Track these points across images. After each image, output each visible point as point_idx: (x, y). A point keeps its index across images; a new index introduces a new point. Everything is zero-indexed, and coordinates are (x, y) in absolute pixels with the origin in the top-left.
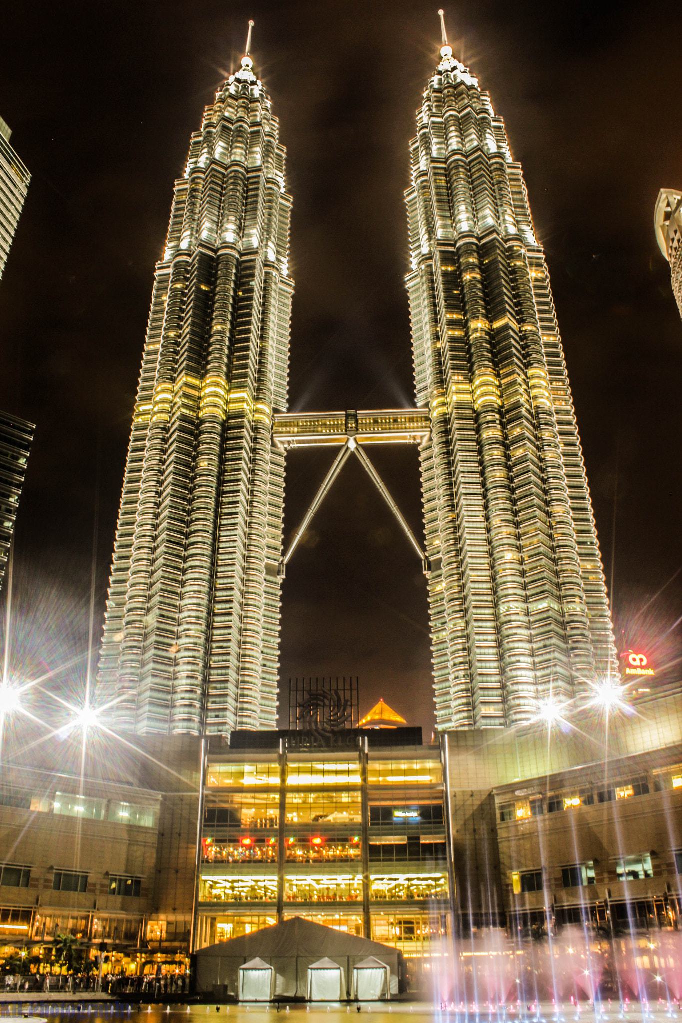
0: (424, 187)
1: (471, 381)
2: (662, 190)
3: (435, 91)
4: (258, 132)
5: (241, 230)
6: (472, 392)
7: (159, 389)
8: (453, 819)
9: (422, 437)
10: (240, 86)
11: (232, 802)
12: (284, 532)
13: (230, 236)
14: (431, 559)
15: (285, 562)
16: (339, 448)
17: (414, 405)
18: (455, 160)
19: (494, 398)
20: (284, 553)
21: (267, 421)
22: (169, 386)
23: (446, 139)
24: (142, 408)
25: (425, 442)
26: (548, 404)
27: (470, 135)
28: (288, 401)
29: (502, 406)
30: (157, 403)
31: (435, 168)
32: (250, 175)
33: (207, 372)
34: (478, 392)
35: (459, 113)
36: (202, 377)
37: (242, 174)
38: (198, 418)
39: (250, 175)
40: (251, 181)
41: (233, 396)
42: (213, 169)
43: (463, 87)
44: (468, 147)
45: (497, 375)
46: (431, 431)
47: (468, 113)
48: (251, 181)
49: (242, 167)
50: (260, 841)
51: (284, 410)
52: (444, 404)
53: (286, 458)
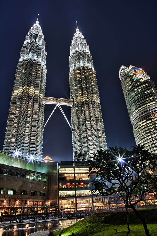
1: (83, 95)
3: (76, 37)
4: (41, 38)
5: (38, 57)
6: (83, 97)
7: (19, 88)
8: (57, 179)
9: (71, 105)
10: (37, 27)
11: (64, 176)
13: (35, 58)
16: (56, 105)
17: (70, 98)
18: (80, 52)
19: (87, 99)
20: (44, 125)
21: (42, 98)
23: (78, 47)
24: (15, 92)
25: (71, 106)
26: (96, 101)
27: (83, 47)
29: (88, 101)
30: (19, 91)
32: (39, 46)
33: (31, 86)
34: (84, 97)
35: (81, 43)
36: (30, 87)
37: (38, 46)
38: (29, 95)
39: (39, 46)
40: (40, 48)
41: (35, 92)
42: (32, 44)
43: (81, 38)
44: (82, 50)
45: (88, 95)
46: (74, 104)
47: (83, 43)
48: (40, 48)
50: (71, 184)
52: (77, 99)
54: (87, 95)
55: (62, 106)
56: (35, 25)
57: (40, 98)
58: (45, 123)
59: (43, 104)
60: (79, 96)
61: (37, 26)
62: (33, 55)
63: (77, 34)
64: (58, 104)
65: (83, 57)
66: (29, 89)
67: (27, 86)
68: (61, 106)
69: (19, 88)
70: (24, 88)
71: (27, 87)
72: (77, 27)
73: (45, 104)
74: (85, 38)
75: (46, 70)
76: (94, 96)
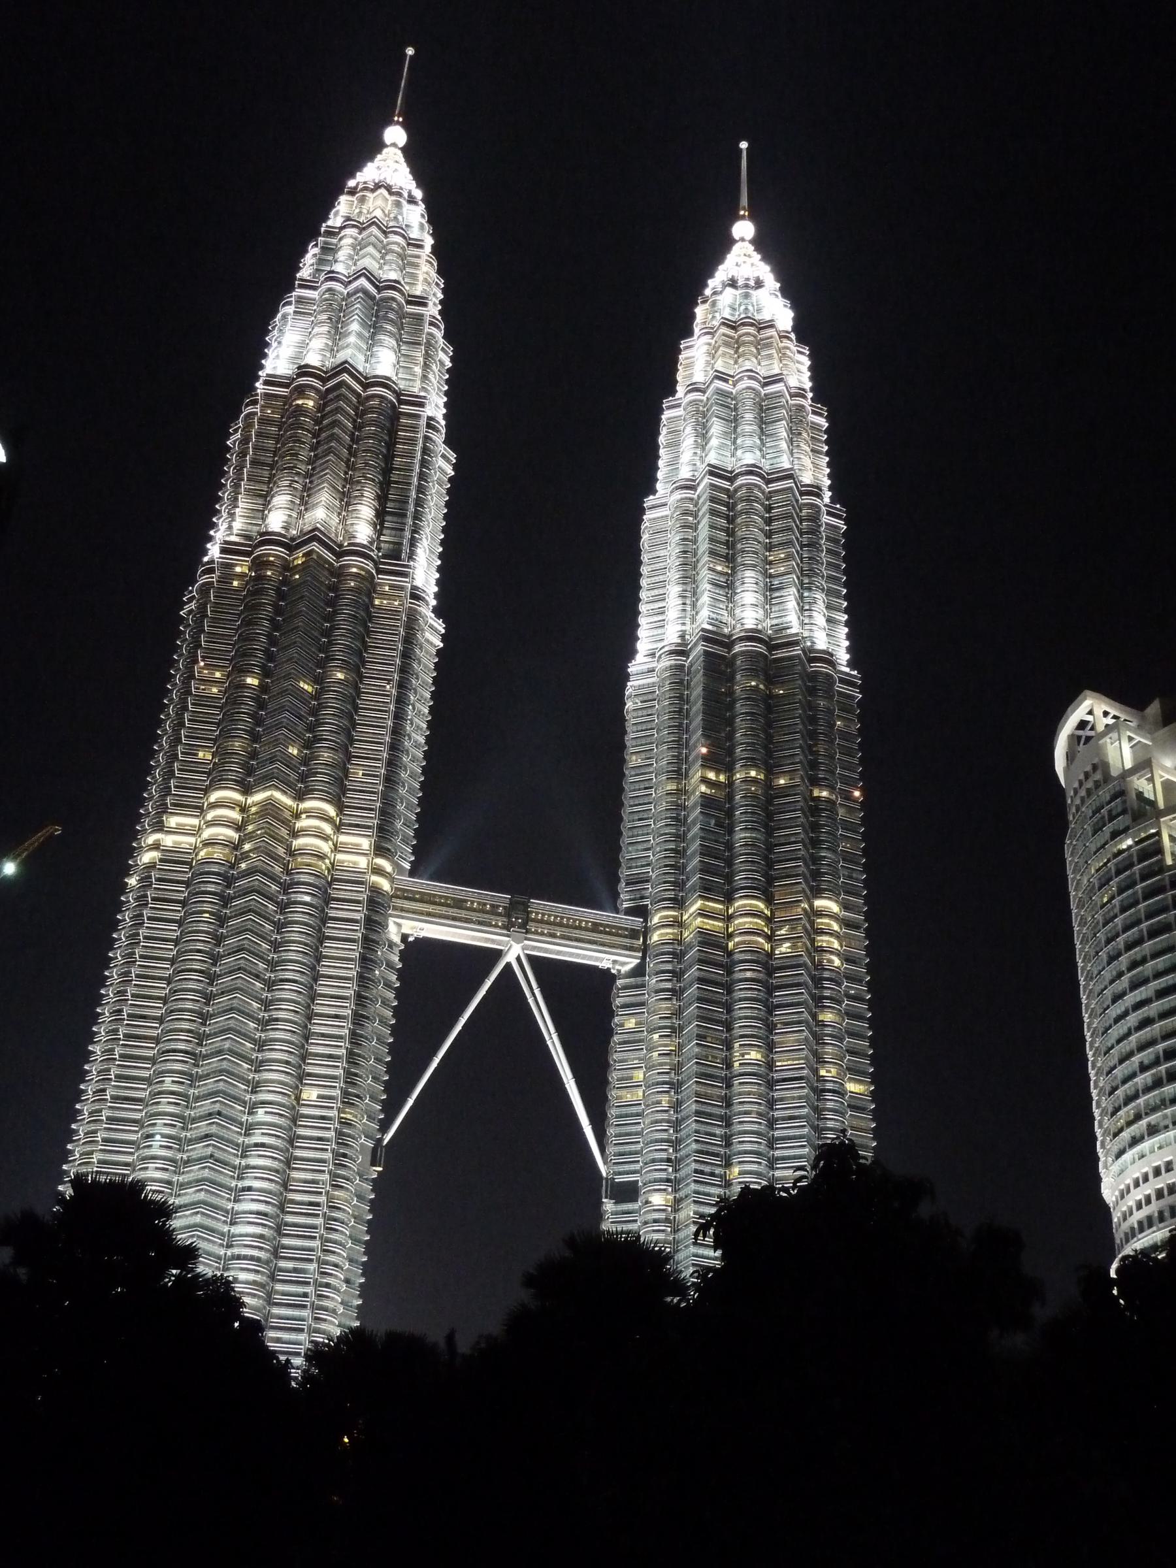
0: (686, 513)
2: (1088, 692)
6: (729, 918)
12: (388, 1087)
14: (619, 1179)
15: (385, 1142)
18: (750, 487)
20: (384, 1126)
21: (385, 885)
22: (237, 796)
28: (416, 851)
31: (713, 486)
32: (405, 408)
36: (300, 797)
39: (405, 408)
41: (343, 838)
43: (771, 332)
46: (643, 958)
49: (394, 392)
51: (407, 866)
53: (403, 955)
54: (761, 905)
55: (542, 967)
56: (369, 173)
57: (375, 890)
58: (391, 1108)
59: (391, 945)
60: (699, 903)
61: (389, 188)
62: (346, 501)
63: (733, 283)
64: (514, 951)
65: (769, 535)
66: (297, 816)
67: (277, 788)
68: (537, 963)
69: (214, 796)
70: (259, 797)
71: (278, 795)
72: (744, 200)
73: (404, 938)
74: (803, 331)
75: (440, 626)
76: (820, 914)
